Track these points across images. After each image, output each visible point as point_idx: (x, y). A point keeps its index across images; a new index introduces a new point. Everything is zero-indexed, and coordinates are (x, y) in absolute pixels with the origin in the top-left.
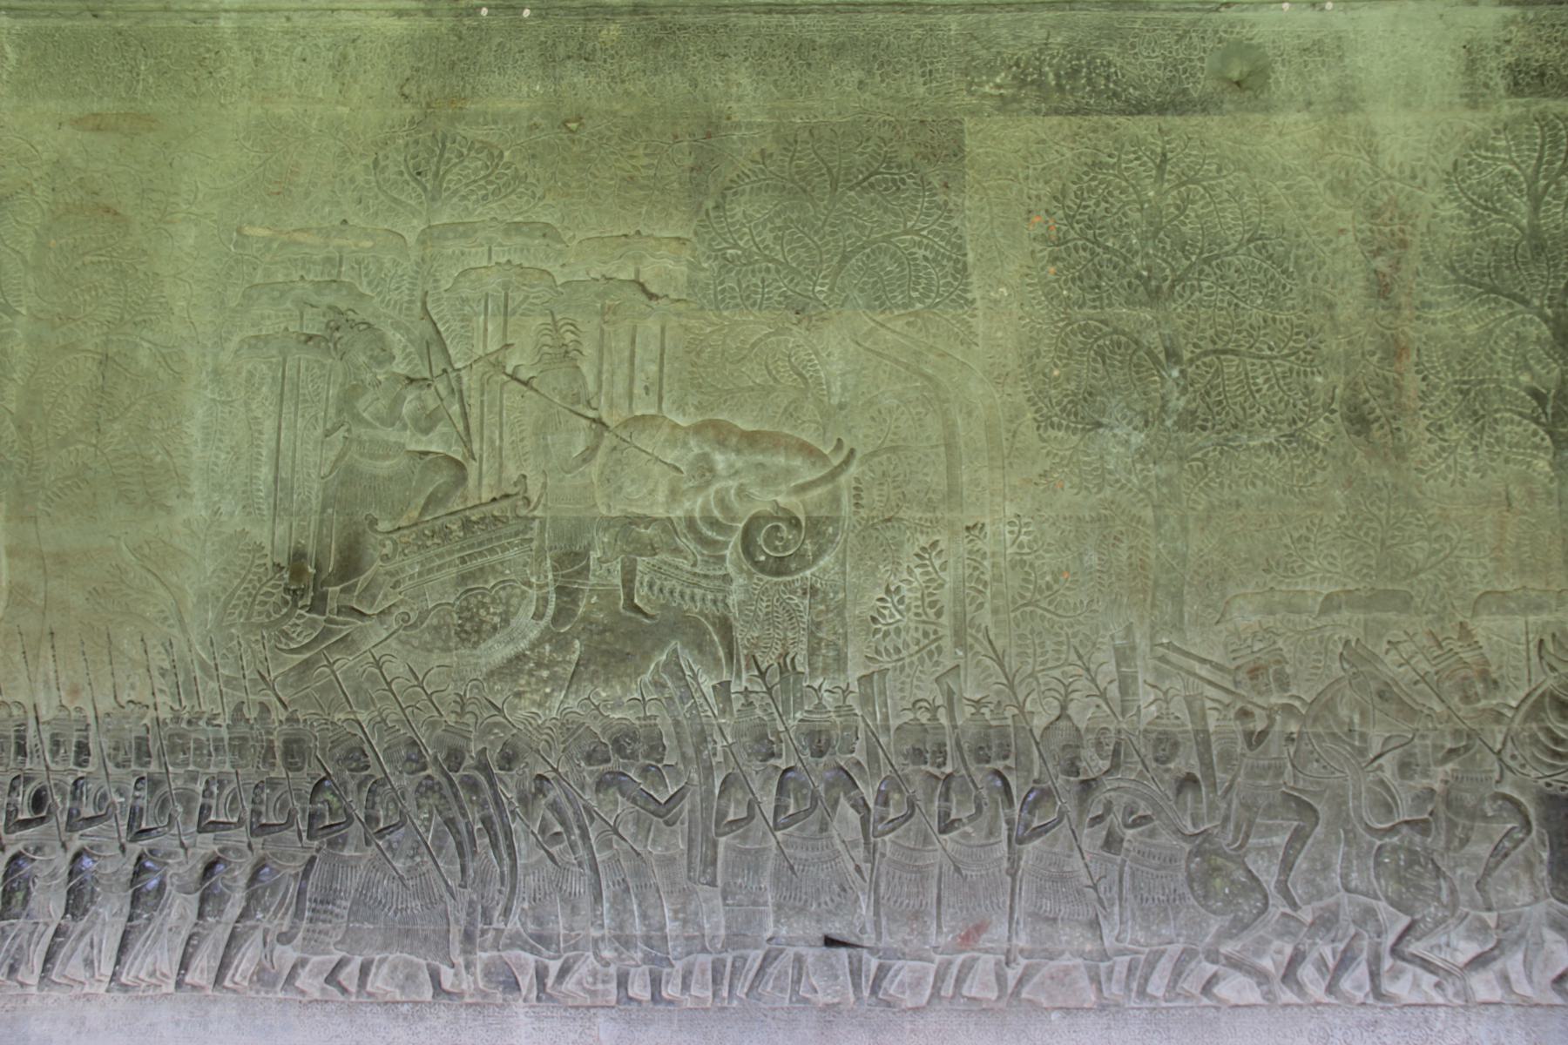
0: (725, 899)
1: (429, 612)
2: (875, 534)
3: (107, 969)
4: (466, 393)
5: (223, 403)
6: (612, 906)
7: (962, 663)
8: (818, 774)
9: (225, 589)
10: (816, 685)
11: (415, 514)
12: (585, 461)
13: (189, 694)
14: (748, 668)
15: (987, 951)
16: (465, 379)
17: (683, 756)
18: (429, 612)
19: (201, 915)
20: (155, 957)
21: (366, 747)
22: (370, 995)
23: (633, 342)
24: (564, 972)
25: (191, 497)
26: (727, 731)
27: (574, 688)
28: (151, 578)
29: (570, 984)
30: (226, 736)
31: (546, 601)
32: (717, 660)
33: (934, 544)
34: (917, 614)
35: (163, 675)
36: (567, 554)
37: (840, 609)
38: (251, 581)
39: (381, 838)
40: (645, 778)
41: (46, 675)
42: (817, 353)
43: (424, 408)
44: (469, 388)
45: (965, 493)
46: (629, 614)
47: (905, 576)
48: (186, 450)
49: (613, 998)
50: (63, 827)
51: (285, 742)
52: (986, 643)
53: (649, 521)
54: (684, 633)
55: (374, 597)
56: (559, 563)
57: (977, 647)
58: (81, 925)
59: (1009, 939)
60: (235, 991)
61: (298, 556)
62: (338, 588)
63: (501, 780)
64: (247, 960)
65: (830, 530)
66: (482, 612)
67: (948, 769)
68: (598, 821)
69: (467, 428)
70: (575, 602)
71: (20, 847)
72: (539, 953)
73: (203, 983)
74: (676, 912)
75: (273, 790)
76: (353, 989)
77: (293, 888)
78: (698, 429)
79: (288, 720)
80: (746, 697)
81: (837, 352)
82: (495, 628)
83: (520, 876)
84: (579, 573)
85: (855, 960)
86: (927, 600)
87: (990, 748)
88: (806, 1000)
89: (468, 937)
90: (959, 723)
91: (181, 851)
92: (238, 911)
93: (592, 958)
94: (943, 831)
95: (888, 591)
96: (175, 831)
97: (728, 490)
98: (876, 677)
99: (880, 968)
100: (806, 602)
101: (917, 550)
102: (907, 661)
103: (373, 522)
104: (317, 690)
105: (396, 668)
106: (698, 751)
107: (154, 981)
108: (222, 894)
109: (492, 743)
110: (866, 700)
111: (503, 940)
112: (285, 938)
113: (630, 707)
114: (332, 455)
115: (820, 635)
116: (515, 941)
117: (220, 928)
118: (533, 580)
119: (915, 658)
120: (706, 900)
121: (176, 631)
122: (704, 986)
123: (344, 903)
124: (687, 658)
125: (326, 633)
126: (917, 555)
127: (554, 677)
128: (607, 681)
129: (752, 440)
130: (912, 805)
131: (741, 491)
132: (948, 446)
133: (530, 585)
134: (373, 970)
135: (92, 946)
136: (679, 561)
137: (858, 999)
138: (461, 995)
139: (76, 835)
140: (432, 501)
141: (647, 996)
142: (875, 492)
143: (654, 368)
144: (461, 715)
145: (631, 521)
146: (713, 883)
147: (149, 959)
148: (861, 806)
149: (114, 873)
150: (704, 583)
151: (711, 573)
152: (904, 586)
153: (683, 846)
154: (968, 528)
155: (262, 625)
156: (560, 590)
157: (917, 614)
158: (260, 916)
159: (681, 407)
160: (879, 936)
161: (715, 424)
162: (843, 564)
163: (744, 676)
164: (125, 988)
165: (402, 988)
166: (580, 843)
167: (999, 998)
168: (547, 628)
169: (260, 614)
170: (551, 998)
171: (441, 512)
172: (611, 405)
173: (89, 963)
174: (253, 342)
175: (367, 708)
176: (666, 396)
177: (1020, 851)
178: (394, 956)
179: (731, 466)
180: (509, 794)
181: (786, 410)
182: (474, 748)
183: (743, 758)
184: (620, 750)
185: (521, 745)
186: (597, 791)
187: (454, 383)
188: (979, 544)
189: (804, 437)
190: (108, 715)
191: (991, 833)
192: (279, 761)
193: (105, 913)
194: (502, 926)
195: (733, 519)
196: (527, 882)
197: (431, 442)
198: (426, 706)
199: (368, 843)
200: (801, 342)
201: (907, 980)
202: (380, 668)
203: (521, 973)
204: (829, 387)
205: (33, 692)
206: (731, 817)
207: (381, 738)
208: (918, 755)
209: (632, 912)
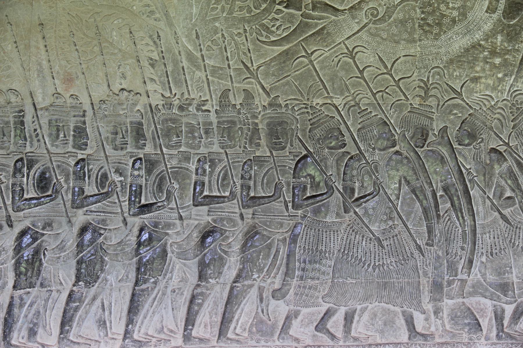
13: (177, 83)
19: (202, 276)
20: (161, 317)
21: (343, 127)
22: (356, 339)
35: (152, 65)
39: (359, 206)
41: (40, 64)
50: (69, 204)
51: (268, 125)
58: (93, 290)
60: (238, 341)
63: (460, 153)
71: (27, 223)
72: (499, 299)
73: (207, 336)
75: (260, 167)
76: (339, 334)
77: (283, 251)
79: (270, 105)
82: (454, 21)
89: (437, 287)
91: (178, 222)
92: (234, 273)
96: (173, 205)
104: (296, 78)
105: (367, 57)
109: (452, 122)
111: (467, 289)
116: (477, 290)
121: (162, 24)
123: (329, 262)
125: (303, 27)
134: (356, 317)
135: (104, 310)
138: (432, 336)
139: (80, 212)
144: (424, 98)
147: (156, 318)
155: (243, 20)
158: (255, 276)
165: (382, 332)
168: (499, 20)
169: (241, 8)
173: (102, 324)
175: (342, 94)
178: (374, 306)
182: (437, 126)
185: (478, 123)
190: (103, 101)
192: (263, 142)
193: (111, 278)
194: (465, 277)
196: (485, 240)
198: (395, 92)
202: (353, 58)
203: (482, 316)
205: (27, 80)
207: (355, 120)
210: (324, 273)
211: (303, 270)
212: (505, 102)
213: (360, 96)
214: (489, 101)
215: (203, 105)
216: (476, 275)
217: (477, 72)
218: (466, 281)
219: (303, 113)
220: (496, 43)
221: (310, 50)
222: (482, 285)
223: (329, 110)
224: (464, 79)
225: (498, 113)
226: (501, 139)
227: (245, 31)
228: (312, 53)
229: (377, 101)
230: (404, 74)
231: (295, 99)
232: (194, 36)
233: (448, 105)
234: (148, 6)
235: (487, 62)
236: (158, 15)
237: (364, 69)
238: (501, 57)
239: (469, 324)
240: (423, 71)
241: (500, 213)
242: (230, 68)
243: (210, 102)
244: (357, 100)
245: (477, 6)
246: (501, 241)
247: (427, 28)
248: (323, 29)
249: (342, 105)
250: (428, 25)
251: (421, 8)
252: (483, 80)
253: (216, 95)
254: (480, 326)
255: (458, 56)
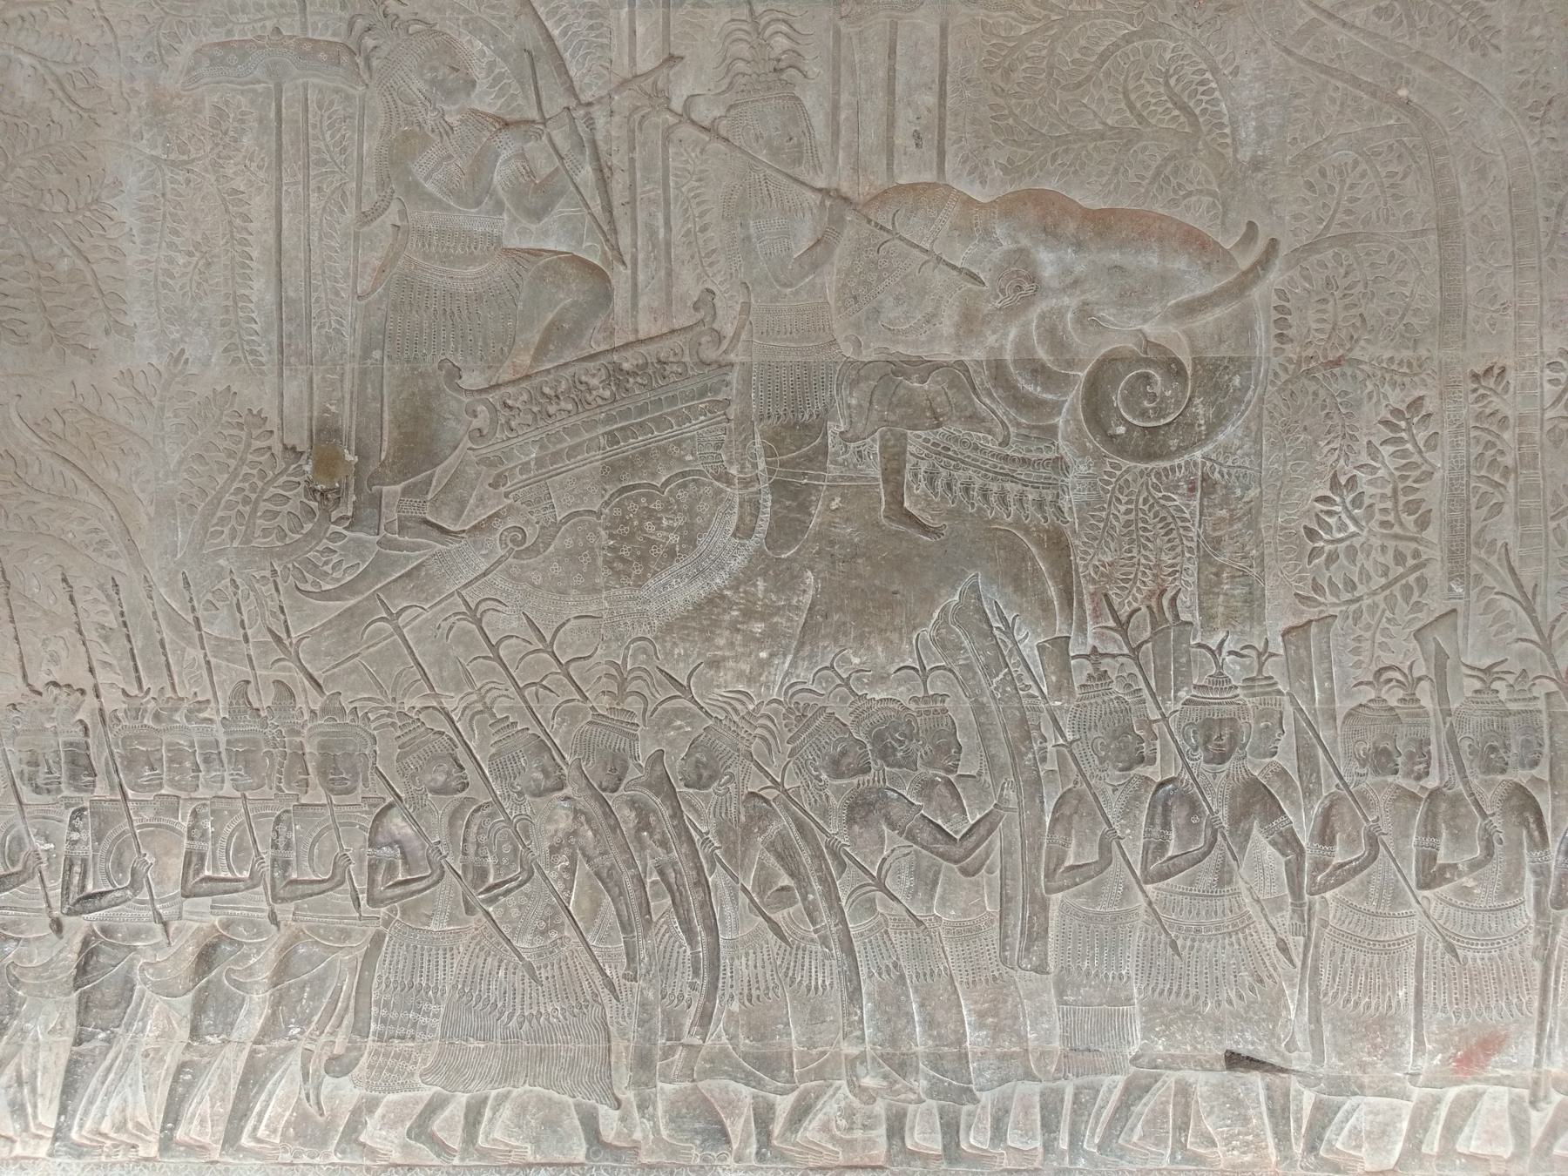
0: (1061, 993)
1: (557, 526)
2: (1312, 387)
3: (47, 1116)
4: (602, 146)
5: (173, 164)
6: (877, 1007)
7: (1460, 605)
8: (1216, 792)
9: (203, 492)
10: (1213, 643)
11: (526, 359)
12: (815, 266)
14: (1097, 616)
15: (1499, 1082)
16: (601, 122)
17: (991, 759)
18: (557, 526)
19: (195, 1032)
20: (127, 1100)
21: (460, 752)
22: (484, 1154)
23: (892, 51)
24: (800, 1113)
25: (130, 333)
26: (1065, 722)
27: (808, 648)
28: (70, 474)
29: (810, 1130)
30: (223, 739)
31: (756, 506)
32: (1046, 605)
33: (1417, 404)
34: (1384, 524)
35: (106, 639)
36: (790, 427)
37: (1252, 515)
38: (247, 477)
40: (929, 799)
42: (1215, 71)
43: (530, 173)
44: (608, 139)
45: (1472, 314)
46: (895, 527)
47: (1364, 458)
48: (115, 250)
49: (880, 1151)
51: (323, 746)
52: (1504, 573)
53: (928, 368)
54: (990, 559)
55: (463, 503)
56: (775, 443)
57: (1489, 580)
59: (1538, 1064)
60: (258, 1155)
61: (326, 437)
62: (399, 488)
64: (278, 1100)
65: (1237, 380)
66: (649, 526)
67: (1432, 782)
68: (852, 869)
69: (608, 208)
70: (804, 508)
72: (759, 1084)
73: (206, 1140)
74: (981, 1015)
76: (455, 1143)
77: (348, 984)
78: (1009, 207)
79: (324, 710)
80: (1096, 664)
81: (1250, 66)
83: (725, 960)
84: (809, 459)
85: (1278, 1095)
86: (1402, 499)
87: (1507, 748)
88: (1197, 1159)
89: (643, 1061)
90: (1454, 706)
91: (158, 927)
93: (845, 1089)
94: (1423, 885)
95: (1334, 484)
97: (1061, 313)
98: (1314, 629)
99: (1318, 1106)
100: (1196, 503)
101: (1385, 414)
102: (1366, 602)
103: (455, 373)
105: (504, 621)
106: (1016, 755)
107: (124, 1137)
108: (229, 998)
109: (671, 743)
110: (1298, 669)
112: (338, 1066)
113: (900, 682)
114: (375, 259)
115: (1220, 560)
116: (718, 1064)
117: (229, 1051)
118: (733, 471)
119: (1379, 598)
120: (1030, 996)
121: (122, 564)
122: (1027, 1134)
124: (994, 597)
126: (1386, 423)
127: (773, 633)
128: (861, 638)
129: (1102, 224)
130: (1373, 842)
131: (1085, 315)
132: (1444, 233)
133: (728, 481)
134: (488, 1113)
136: (978, 436)
137: (1286, 1156)
138: (635, 1149)
140: (556, 336)
141: (936, 1146)
142: (1311, 314)
143: (930, 99)
144: (622, 693)
145: (898, 369)
146: (1041, 969)
147: (114, 1103)
148: (1288, 842)
149: (45, 966)
150: (1022, 472)
151: (1033, 456)
152: (1362, 476)
153: (992, 908)
154: (1475, 377)
155: (269, 552)
156: (777, 486)
157: (1384, 524)
159: (977, 172)
160: (1319, 1056)
161: (1038, 198)
162: (1257, 441)
163: (1091, 628)
164: (78, 1151)
165: (537, 1142)
166: (822, 905)
167: (1517, 1157)
169: (266, 532)
170: (781, 1156)
171: (569, 355)
172: (857, 168)
174: (219, 53)
175: (458, 688)
176: (950, 150)
177: (1557, 919)
179: (1067, 271)
180: (703, 827)
181: (1158, 173)
182: (644, 750)
183: (1091, 765)
184: (885, 754)
186: (851, 821)
187: (582, 128)
188: (1496, 403)
189: (1188, 220)
191: (1507, 890)
193: (37, 1029)
194: (697, 1041)
195: (1070, 364)
196: (739, 967)
197: (545, 233)
199: (469, 910)
200: (1188, 50)
201: (1365, 1126)
202: (478, 623)
204: (1234, 131)
206: (1070, 862)
207: (484, 738)
208: (1382, 760)
209: (909, 1015)
210: (424, 1028)
211: (384, 1021)
212: (774, 705)
213: (495, 693)
214: (743, 703)
215: (199, 711)
216: (719, 1037)
217: (719, 648)
218: (698, 1048)
219: (386, 725)
220: (754, 595)
221: (395, 606)
222: (728, 1056)
223: (434, 720)
224: (694, 660)
225: (762, 726)
226: (767, 774)
227: (275, 571)
228: (399, 614)
229: (526, 702)
230: (577, 651)
231: (369, 699)
232: (181, 584)
233: (666, 711)
234: (96, 530)
235: (738, 630)
236: (114, 548)
237: (501, 641)
238: (763, 620)
239: (703, 1131)
240: (614, 646)
241: (768, 919)
242: (247, 641)
243: (213, 704)
244: (488, 701)
245: (715, 525)
246: (769, 973)
247: (619, 566)
248: (417, 568)
249: (459, 711)
250: (623, 560)
251: (606, 528)
252: (731, 664)
253: (225, 691)
254: (726, 1134)
255: (683, 618)
